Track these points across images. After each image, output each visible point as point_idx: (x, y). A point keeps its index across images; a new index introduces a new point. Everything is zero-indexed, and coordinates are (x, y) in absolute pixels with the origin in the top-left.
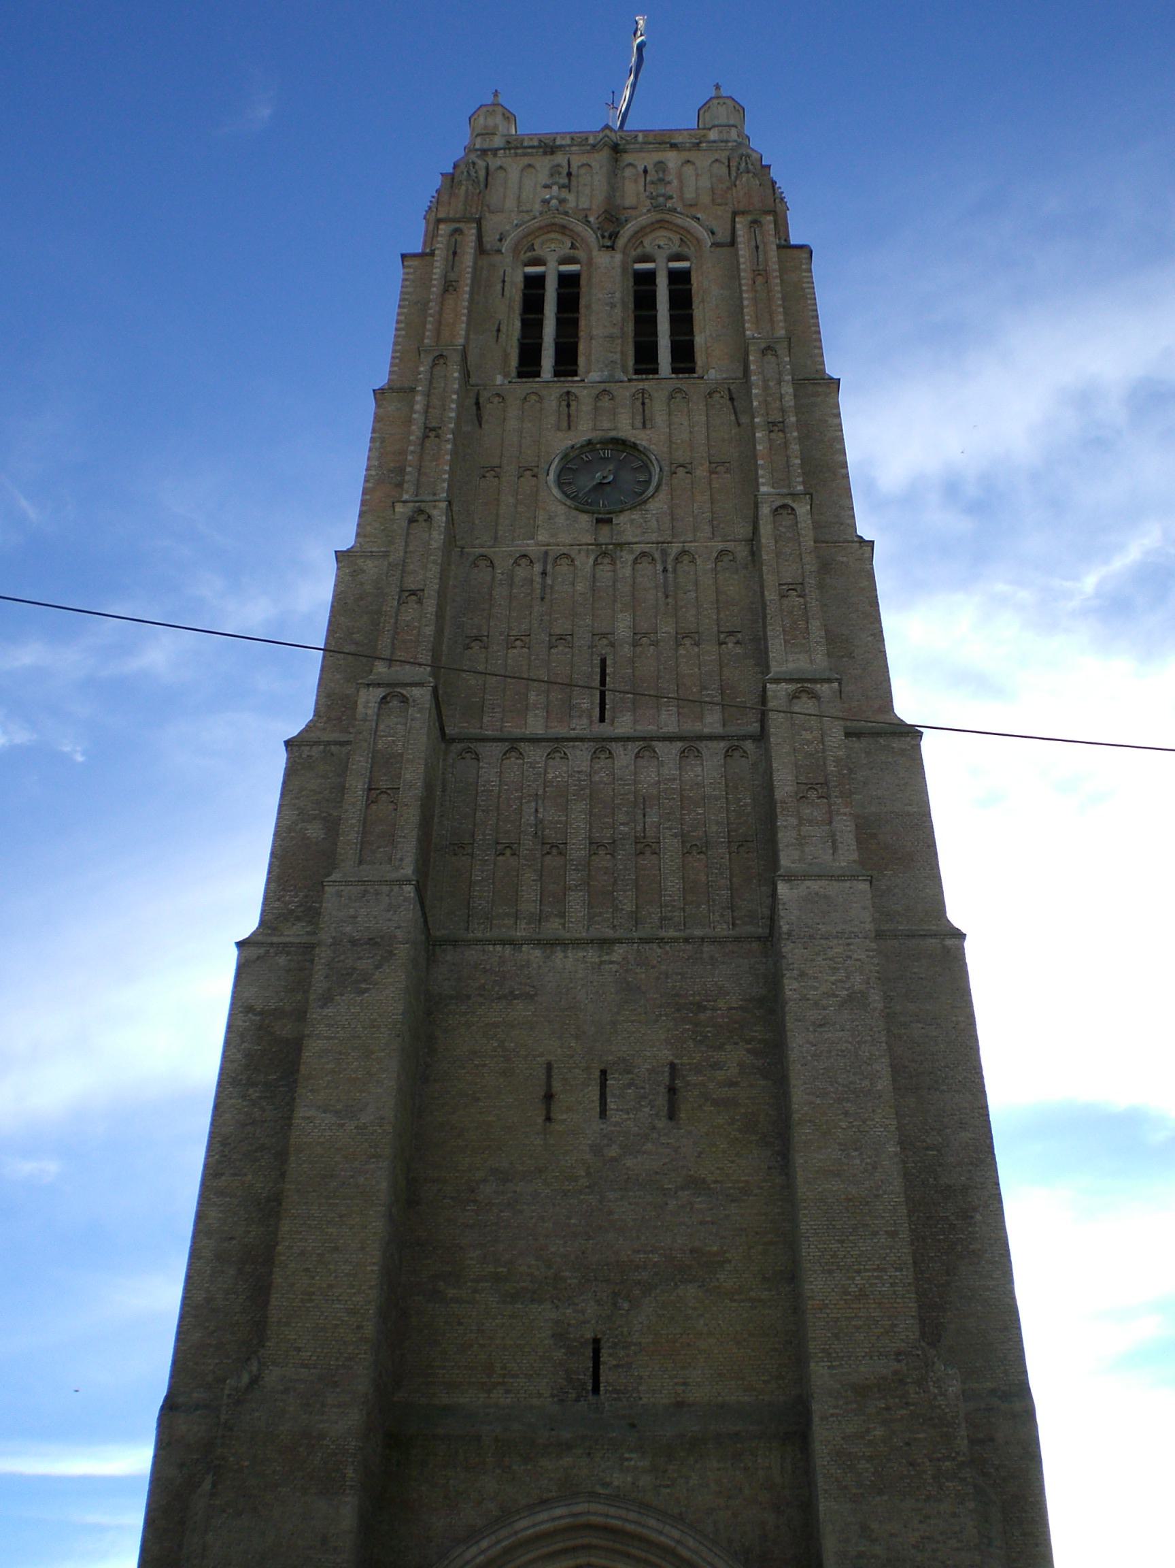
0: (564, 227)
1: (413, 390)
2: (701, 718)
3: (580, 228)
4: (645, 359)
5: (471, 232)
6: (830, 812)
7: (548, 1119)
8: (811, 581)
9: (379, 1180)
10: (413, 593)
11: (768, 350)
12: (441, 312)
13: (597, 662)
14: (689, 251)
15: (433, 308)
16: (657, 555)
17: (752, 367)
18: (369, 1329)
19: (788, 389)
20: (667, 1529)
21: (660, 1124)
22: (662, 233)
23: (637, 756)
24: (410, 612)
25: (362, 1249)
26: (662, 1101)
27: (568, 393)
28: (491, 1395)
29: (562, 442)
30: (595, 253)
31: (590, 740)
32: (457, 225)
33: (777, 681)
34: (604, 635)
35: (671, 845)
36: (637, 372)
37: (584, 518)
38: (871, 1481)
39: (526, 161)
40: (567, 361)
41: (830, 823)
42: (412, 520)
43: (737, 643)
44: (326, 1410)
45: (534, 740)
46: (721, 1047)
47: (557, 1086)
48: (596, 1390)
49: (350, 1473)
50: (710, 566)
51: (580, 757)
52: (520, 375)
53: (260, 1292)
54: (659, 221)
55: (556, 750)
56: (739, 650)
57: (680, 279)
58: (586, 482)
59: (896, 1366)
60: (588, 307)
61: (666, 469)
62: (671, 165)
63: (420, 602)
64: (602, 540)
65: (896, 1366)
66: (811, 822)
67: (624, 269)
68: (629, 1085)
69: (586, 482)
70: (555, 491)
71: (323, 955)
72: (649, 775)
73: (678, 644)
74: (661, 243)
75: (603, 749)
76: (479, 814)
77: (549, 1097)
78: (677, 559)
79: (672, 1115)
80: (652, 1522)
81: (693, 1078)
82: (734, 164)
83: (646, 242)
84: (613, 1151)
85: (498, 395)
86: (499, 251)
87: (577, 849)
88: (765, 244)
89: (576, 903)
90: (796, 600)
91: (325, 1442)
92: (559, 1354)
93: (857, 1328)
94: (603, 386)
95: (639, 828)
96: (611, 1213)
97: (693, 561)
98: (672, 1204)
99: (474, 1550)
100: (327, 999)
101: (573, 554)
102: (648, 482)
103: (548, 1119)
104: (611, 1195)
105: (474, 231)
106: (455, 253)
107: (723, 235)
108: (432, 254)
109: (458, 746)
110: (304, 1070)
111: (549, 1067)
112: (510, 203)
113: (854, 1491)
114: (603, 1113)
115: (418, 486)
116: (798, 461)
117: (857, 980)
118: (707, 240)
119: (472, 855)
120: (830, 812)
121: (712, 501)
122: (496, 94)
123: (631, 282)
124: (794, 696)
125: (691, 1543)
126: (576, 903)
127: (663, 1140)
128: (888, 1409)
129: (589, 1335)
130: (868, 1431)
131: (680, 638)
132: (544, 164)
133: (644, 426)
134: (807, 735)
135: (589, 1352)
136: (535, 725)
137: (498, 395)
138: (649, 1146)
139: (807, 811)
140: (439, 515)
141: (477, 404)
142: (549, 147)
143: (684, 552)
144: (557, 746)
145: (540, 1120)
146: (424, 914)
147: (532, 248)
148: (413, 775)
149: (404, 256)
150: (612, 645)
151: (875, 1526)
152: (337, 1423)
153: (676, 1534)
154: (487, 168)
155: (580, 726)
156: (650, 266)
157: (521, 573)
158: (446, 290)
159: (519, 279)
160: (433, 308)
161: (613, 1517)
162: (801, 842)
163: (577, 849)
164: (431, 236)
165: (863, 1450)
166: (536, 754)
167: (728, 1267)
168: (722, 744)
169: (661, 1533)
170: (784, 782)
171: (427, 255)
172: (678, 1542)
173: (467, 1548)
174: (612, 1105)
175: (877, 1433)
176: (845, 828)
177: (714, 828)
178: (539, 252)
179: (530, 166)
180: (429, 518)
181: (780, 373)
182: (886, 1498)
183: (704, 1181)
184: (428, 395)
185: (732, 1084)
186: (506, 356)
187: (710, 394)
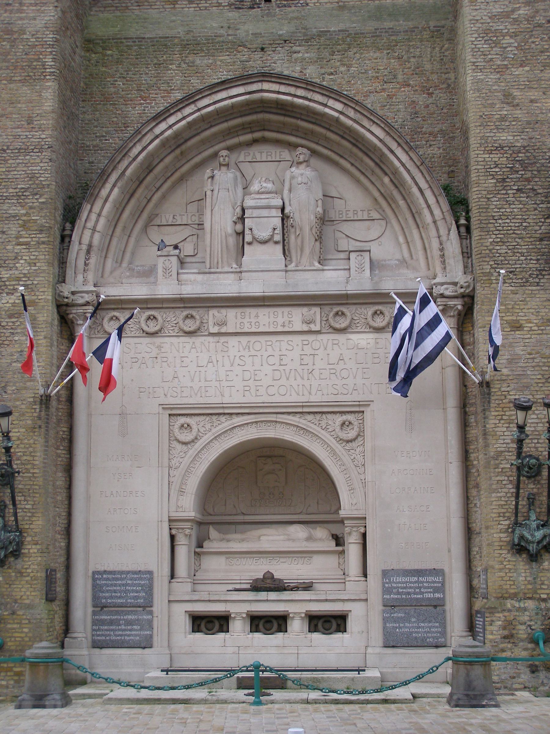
20: (331, 103)
28: (177, 6)
38: (515, 54)
44: (25, 8)
49: (49, 60)
91: (25, 37)
99: (163, 126)
113: (499, 63)
125: (351, 113)
130: (513, 11)
151: (516, 93)
152: (35, 19)
153: (339, 106)
161: (284, 94)
165: (508, 27)
169: (325, 105)
172: (341, 113)
173: (157, 124)
175: (521, 12)
182: (527, 68)
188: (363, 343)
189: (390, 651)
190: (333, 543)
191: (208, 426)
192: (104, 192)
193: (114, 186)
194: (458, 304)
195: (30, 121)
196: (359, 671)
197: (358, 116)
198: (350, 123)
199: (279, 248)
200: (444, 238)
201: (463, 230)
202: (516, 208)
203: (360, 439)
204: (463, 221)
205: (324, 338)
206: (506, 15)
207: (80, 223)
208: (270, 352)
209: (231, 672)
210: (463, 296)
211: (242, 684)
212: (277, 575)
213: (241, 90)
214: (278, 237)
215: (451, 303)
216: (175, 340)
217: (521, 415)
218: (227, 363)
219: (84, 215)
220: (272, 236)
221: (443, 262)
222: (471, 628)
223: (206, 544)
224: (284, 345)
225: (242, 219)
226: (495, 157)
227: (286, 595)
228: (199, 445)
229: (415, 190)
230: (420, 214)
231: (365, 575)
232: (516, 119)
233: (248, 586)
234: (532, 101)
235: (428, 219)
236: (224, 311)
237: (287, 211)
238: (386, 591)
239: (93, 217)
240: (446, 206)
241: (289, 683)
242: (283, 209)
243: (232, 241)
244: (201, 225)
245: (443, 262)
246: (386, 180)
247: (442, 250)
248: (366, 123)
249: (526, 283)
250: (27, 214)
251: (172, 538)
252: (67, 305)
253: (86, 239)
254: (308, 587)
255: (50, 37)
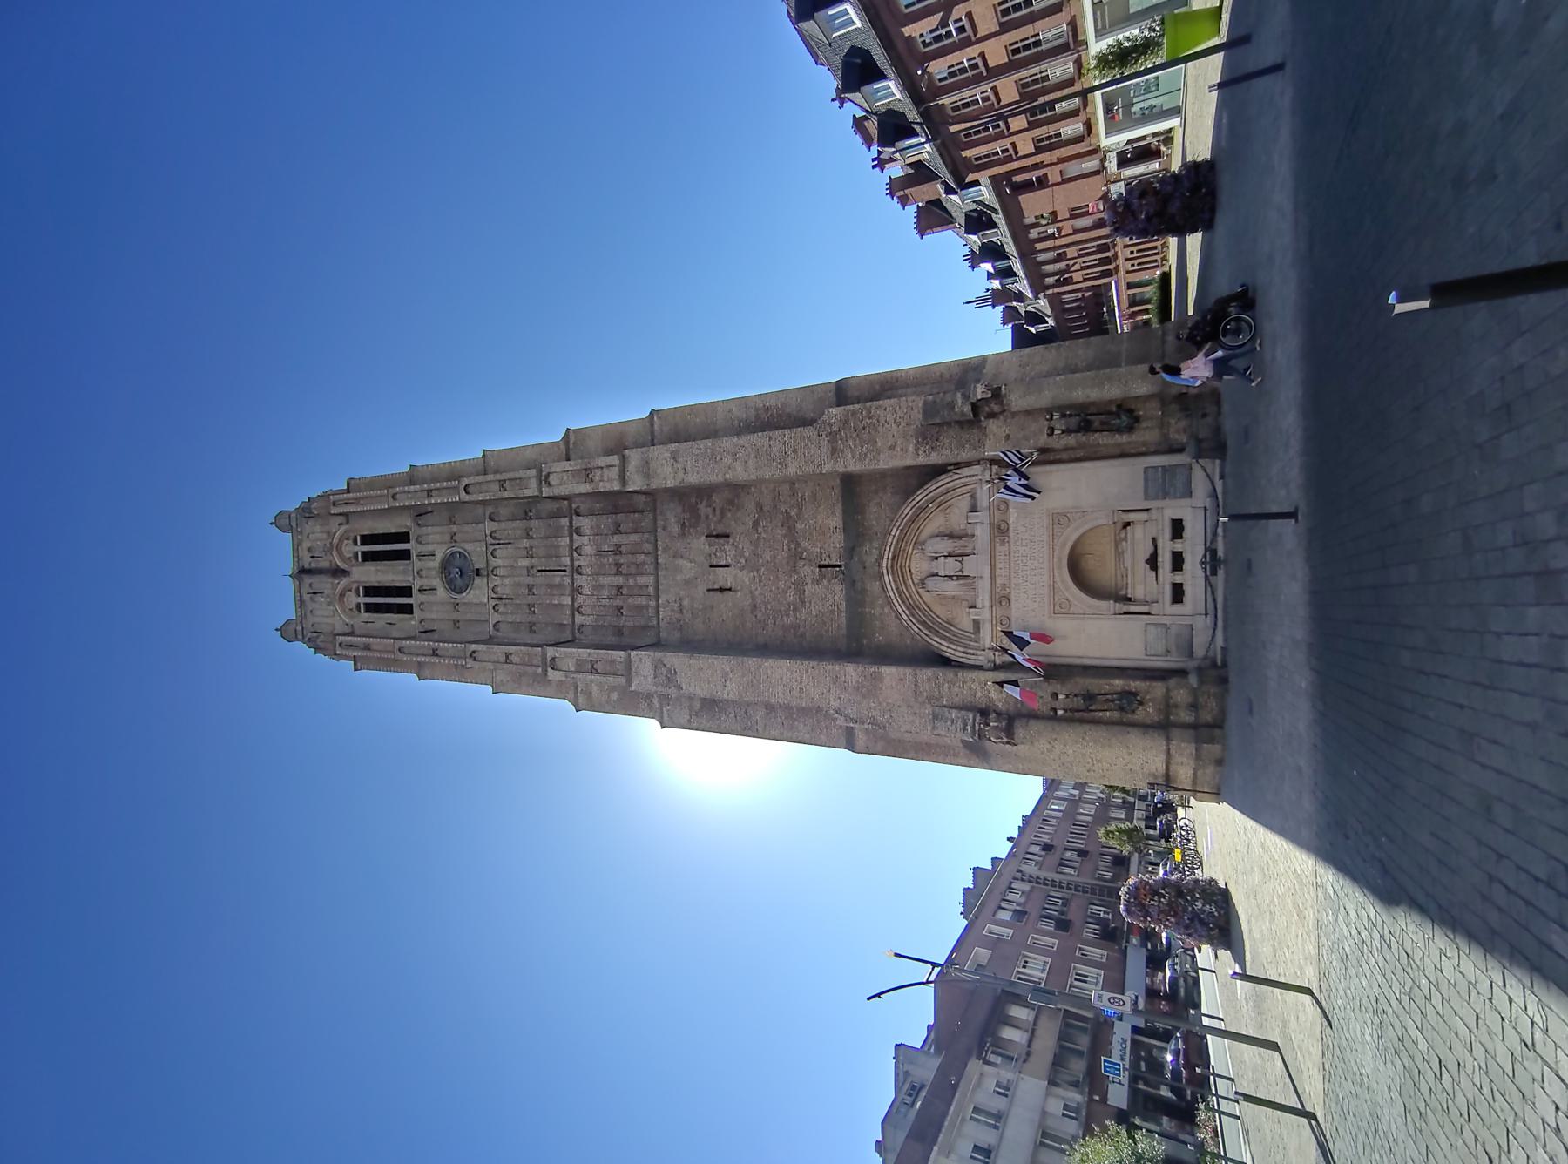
0: (341, 595)
1: (419, 663)
2: (564, 527)
3: (340, 587)
4: (405, 555)
5: (341, 638)
6: (598, 468)
7: (730, 589)
8: (499, 477)
9: (752, 662)
10: (507, 657)
11: (394, 497)
12: (379, 651)
13: (539, 574)
14: (352, 535)
15: (377, 655)
16: (492, 547)
17: (402, 504)
18: (813, 663)
19: (412, 488)
20: (893, 534)
21: (731, 541)
22: (343, 548)
23: (580, 555)
24: (514, 658)
25: (781, 667)
26: (722, 541)
27: (419, 590)
29: (442, 593)
30: (352, 580)
31: (573, 576)
32: (337, 645)
33: (541, 492)
34: (528, 571)
35: (616, 539)
36: (409, 559)
37: (476, 582)
39: (308, 614)
40: (406, 591)
41: (602, 468)
42: (475, 660)
43: (530, 511)
45: (573, 600)
46: (700, 516)
47: (716, 587)
48: (840, 566)
50: (496, 524)
51: (581, 581)
52: (412, 613)
53: (804, 711)
54: (337, 550)
55: (578, 591)
56: (533, 511)
57: (367, 539)
58: (459, 582)
59: (824, 436)
60: (379, 582)
61: (453, 545)
62: (309, 545)
63: (511, 654)
64: (486, 574)
65: (824, 436)
66: (602, 476)
67: (362, 566)
68: (715, 555)
69: (459, 582)
70: (464, 594)
71: (666, 691)
72: (588, 550)
73: (532, 538)
74: (349, 549)
75: (577, 570)
76: (605, 624)
77: (721, 590)
78: (494, 538)
79: (728, 536)
80: (890, 540)
81: (713, 528)
82: (307, 515)
83: (348, 556)
84: (743, 561)
85: (421, 622)
86: (352, 625)
87: (620, 580)
88: (345, 499)
89: (642, 580)
90: (506, 485)
92: (825, 582)
93: (808, 453)
94: (416, 574)
95: (610, 553)
96: (768, 562)
97: (494, 531)
98: (764, 535)
99: (903, 615)
100: (680, 688)
101: (492, 586)
102: (460, 553)
103: (730, 589)
104: (761, 561)
105: (340, 637)
106: (351, 646)
107: (341, 520)
108: (354, 656)
109: (577, 635)
110: (708, 696)
111: (709, 590)
112: (329, 620)
114: (728, 566)
115: (460, 658)
116: (445, 483)
117: (667, 455)
118: (343, 528)
119: (623, 626)
120: (598, 468)
121: (468, 524)
122: (277, 630)
123: (367, 563)
124: (549, 484)
125: (898, 524)
126: (642, 580)
127: (737, 540)
128: (841, 439)
129: (818, 569)
130: (850, 447)
131: (529, 537)
132: (310, 606)
133: (434, 555)
134: (565, 478)
135: (823, 569)
136: (568, 600)
137: (421, 622)
138: (740, 546)
139: (597, 478)
140: (474, 647)
141: (425, 632)
142: (301, 603)
143: (491, 535)
144: (576, 591)
145: (731, 593)
146: (642, 647)
147: (351, 610)
148: (584, 653)
149: (355, 670)
150: (532, 567)
151: (889, 444)
153: (895, 530)
154: (312, 632)
155: (568, 581)
156: (359, 554)
157: (501, 609)
158: (369, 649)
159: (367, 615)
160: (377, 655)
162: (610, 480)
163: (620, 580)
164: (347, 658)
166: (580, 599)
167: (789, 511)
168: (574, 517)
169: (894, 536)
170: (585, 488)
171: (355, 659)
174: (723, 563)
176: (604, 461)
177: (610, 520)
178: (353, 606)
179: (311, 611)
180: (474, 652)
181: (405, 492)
183: (754, 522)
184: (418, 655)
185: (714, 510)
186: (402, 620)
187: (419, 525)
188: (1016, 515)
189: (1193, 494)
190: (1128, 528)
191: (1061, 593)
192: (936, 645)
193: (933, 640)
194: (995, 468)
195: (902, 680)
196: (1205, 509)
197: (900, 520)
198: (903, 524)
199: (965, 558)
200: (961, 476)
201: (956, 467)
202: (947, 441)
203: (1068, 515)
204: (952, 467)
205: (1012, 535)
206: (852, 451)
207: (952, 657)
208: (1020, 562)
209: (1207, 578)
210: (990, 465)
211: (1214, 573)
212: (1147, 557)
213: (886, 577)
214: (960, 559)
215: (994, 471)
216: (1013, 610)
217: (1056, 432)
218: (1025, 584)
219: (948, 655)
220: (960, 561)
221: (973, 476)
222: (1181, 450)
223: (1129, 596)
224: (1017, 555)
225: (950, 577)
226: (920, 452)
227: (1160, 551)
228: (1071, 599)
229: (937, 491)
230: (948, 488)
231: (1147, 510)
232: (902, 444)
233: (1154, 573)
234: (893, 436)
235: (951, 484)
236: (998, 585)
237: (946, 554)
238: (1156, 498)
239: (949, 650)
240: (944, 476)
241: (1213, 547)
242: (945, 556)
243: (961, 582)
244: (953, 597)
245: (973, 476)
246: (931, 506)
247: (967, 477)
248: (903, 516)
249: (985, 434)
250: (948, 682)
251: (1125, 613)
252: (995, 665)
253: (961, 655)
254: (1154, 540)
255: (861, 669)
